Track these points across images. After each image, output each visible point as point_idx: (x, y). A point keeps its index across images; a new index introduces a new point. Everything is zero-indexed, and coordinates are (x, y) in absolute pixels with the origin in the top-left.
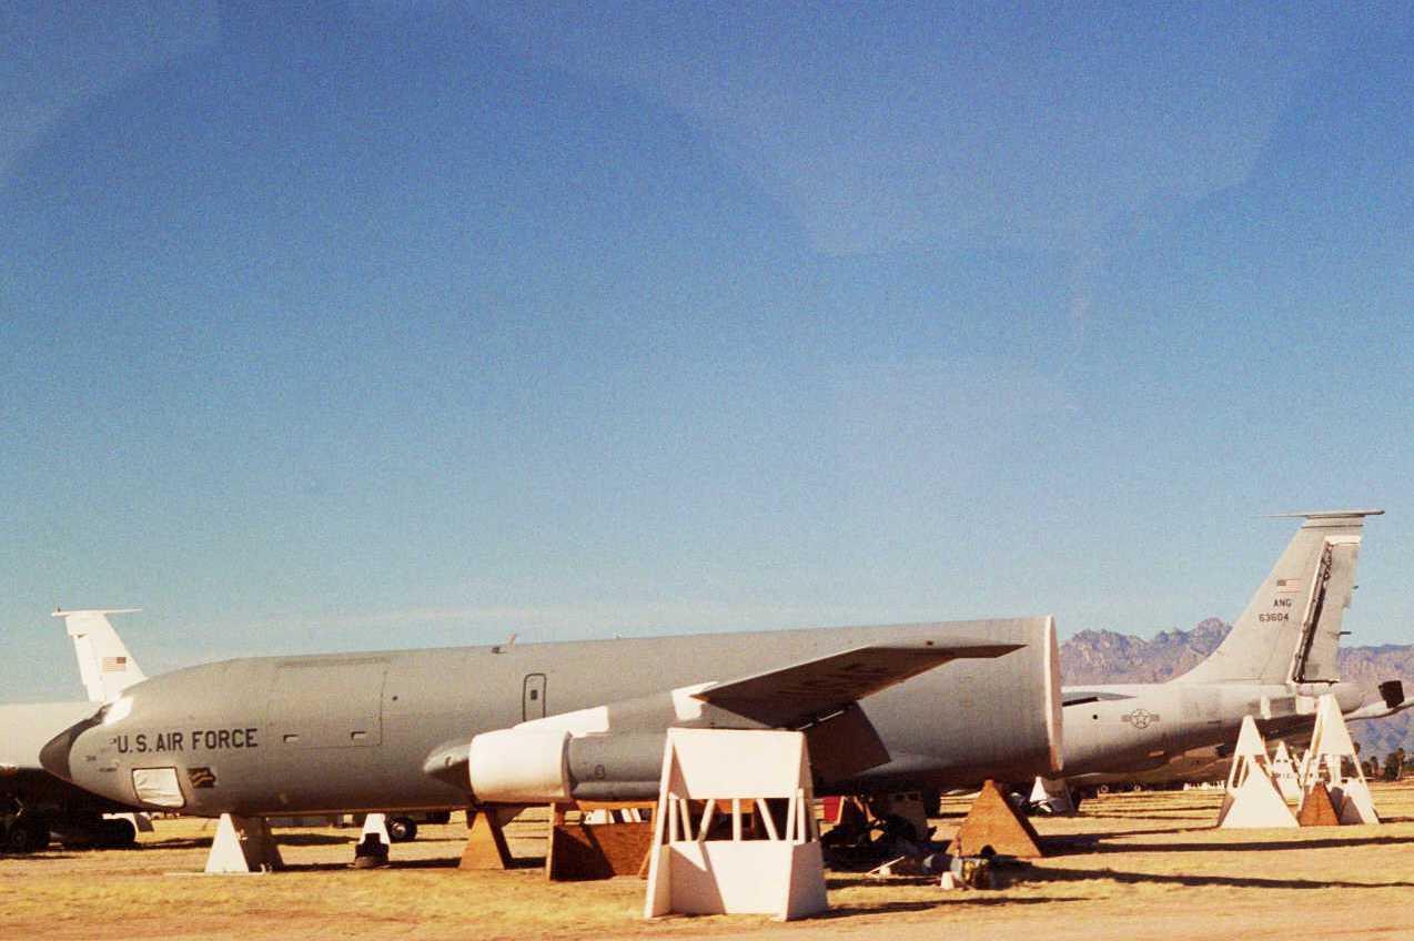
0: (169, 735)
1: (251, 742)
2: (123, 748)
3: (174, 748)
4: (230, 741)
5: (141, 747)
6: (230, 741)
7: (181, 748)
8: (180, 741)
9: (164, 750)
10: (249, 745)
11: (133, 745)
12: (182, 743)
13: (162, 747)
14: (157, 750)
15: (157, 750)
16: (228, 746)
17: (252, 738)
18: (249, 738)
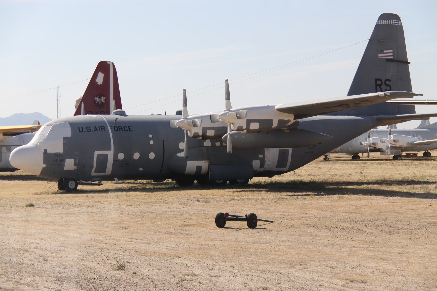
0: (99, 127)
1: (130, 130)
2: (81, 130)
3: (102, 131)
4: (123, 129)
5: (89, 130)
6: (123, 129)
7: (105, 131)
8: (104, 129)
9: (98, 131)
10: (130, 131)
11: (85, 129)
12: (105, 129)
13: (97, 130)
14: (95, 131)
15: (95, 131)
16: (123, 131)
17: (131, 129)
18: (129, 129)
